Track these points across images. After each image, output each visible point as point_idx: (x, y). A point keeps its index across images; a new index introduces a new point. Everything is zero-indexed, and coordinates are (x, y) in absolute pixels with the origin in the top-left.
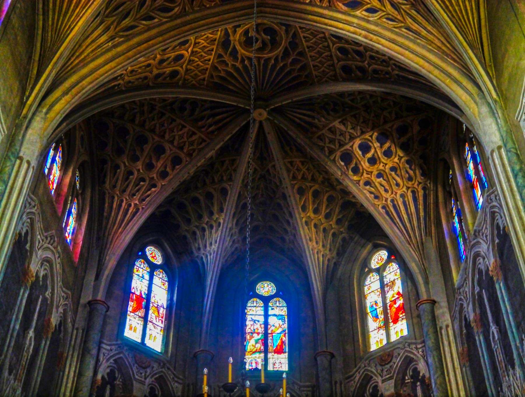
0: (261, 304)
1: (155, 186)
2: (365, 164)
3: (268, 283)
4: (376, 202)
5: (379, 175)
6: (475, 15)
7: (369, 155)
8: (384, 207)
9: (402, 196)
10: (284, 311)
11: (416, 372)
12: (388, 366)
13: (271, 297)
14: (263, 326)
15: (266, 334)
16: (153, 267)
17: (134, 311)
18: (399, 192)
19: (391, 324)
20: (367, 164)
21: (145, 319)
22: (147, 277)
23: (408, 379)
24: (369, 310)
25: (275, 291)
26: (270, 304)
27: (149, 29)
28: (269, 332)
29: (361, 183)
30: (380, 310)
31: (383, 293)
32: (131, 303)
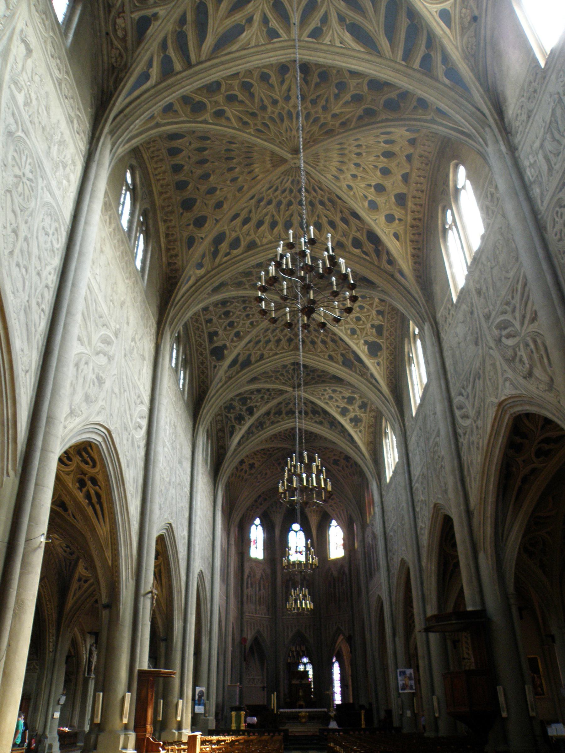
1: (258, 508)
5: (335, 503)
9: (342, 510)
11: (344, 572)
16: (257, 526)
27: (259, 485)
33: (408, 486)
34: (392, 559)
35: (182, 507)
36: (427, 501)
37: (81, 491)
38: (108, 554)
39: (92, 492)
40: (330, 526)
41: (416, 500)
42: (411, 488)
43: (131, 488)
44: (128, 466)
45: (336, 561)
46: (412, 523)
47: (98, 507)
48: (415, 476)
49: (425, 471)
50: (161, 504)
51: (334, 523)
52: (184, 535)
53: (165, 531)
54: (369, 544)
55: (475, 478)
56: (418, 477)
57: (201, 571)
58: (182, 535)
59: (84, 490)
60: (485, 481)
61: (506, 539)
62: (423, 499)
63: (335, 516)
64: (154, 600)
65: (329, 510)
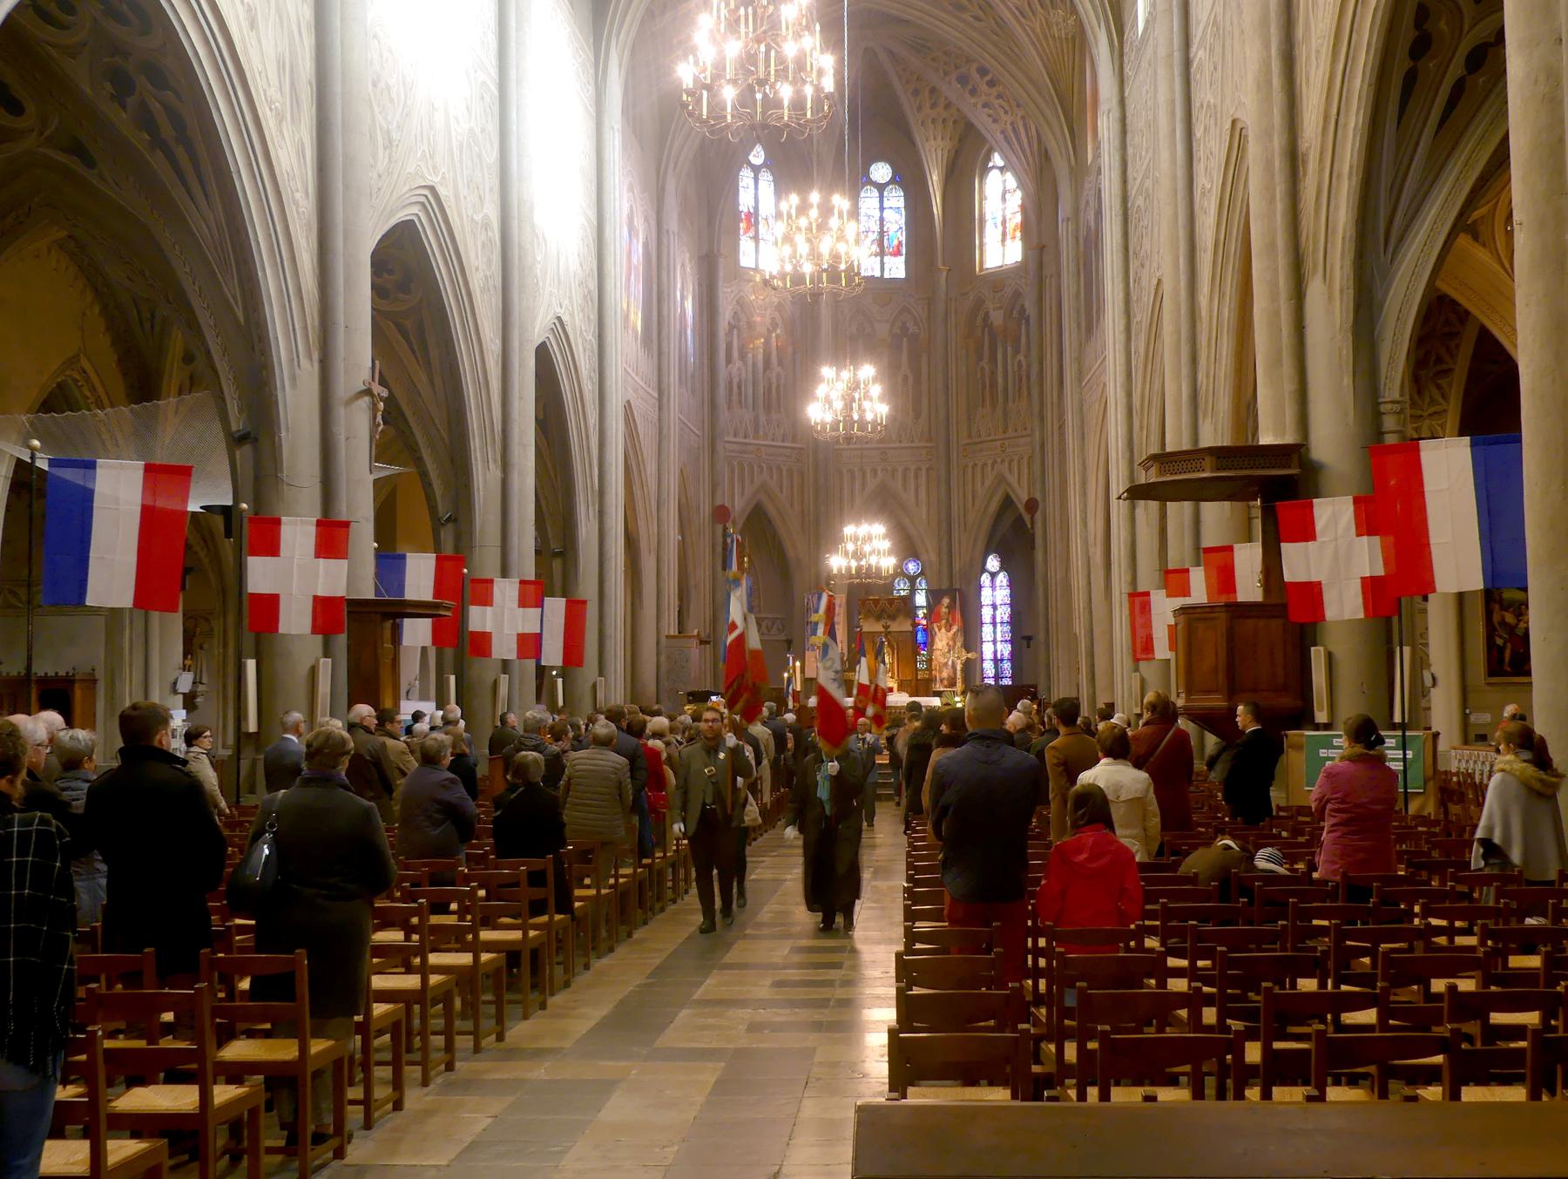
0: (876, 193)
2: (984, 87)
3: (883, 164)
4: (995, 126)
5: (999, 96)
6: (1071, 57)
7: (988, 78)
8: (1003, 132)
10: (901, 203)
11: (1023, 309)
12: (1000, 294)
13: (887, 184)
14: (878, 222)
15: (882, 233)
16: (756, 170)
17: (745, 233)
18: (1020, 114)
19: (1008, 241)
20: (985, 87)
21: (756, 238)
22: (752, 183)
23: (1015, 314)
24: (988, 216)
25: (890, 175)
26: (885, 194)
28: (885, 229)
29: (979, 106)
30: (999, 220)
31: (1004, 199)
32: (742, 225)
33: (1177, 57)
34: (1138, 280)
35: (471, 130)
36: (1219, 109)
37: (124, 107)
38: (231, 290)
39: (156, 107)
40: (985, 170)
41: (1196, 104)
42: (1187, 63)
43: (273, 92)
44: (253, 24)
45: (999, 279)
46: (1181, 172)
47: (180, 152)
48: (1198, 23)
49: (1219, 9)
50: (388, 132)
51: (997, 160)
52: (486, 217)
53: (416, 209)
54: (1089, 228)
55: (1318, 51)
56: (1206, 27)
57: (559, 318)
58: (478, 218)
59: (131, 101)
60: (1341, 66)
61: (1401, 239)
62: (1212, 101)
63: (1000, 137)
64: (379, 415)
65: (981, 120)
